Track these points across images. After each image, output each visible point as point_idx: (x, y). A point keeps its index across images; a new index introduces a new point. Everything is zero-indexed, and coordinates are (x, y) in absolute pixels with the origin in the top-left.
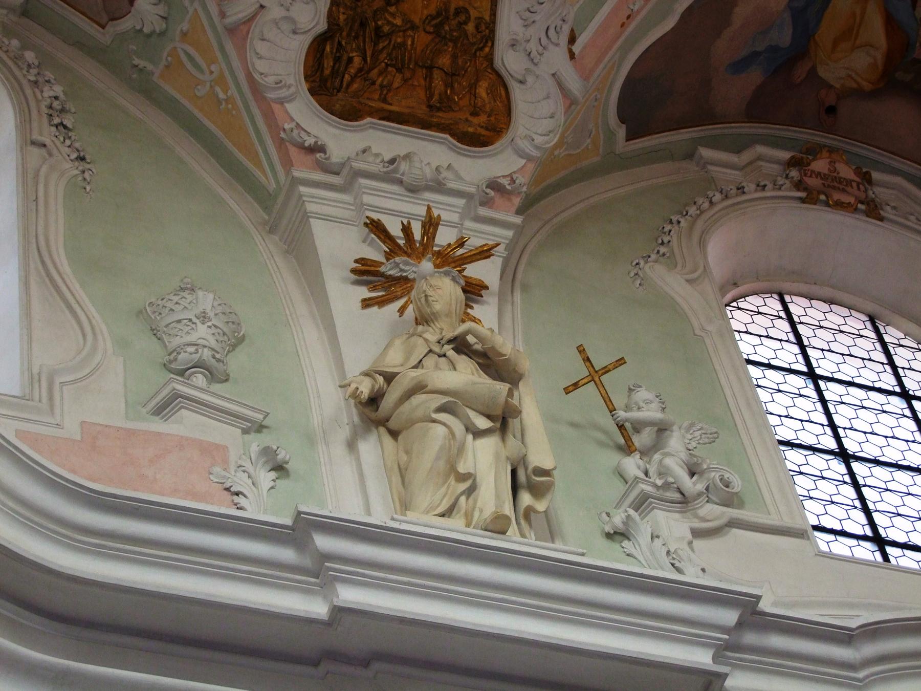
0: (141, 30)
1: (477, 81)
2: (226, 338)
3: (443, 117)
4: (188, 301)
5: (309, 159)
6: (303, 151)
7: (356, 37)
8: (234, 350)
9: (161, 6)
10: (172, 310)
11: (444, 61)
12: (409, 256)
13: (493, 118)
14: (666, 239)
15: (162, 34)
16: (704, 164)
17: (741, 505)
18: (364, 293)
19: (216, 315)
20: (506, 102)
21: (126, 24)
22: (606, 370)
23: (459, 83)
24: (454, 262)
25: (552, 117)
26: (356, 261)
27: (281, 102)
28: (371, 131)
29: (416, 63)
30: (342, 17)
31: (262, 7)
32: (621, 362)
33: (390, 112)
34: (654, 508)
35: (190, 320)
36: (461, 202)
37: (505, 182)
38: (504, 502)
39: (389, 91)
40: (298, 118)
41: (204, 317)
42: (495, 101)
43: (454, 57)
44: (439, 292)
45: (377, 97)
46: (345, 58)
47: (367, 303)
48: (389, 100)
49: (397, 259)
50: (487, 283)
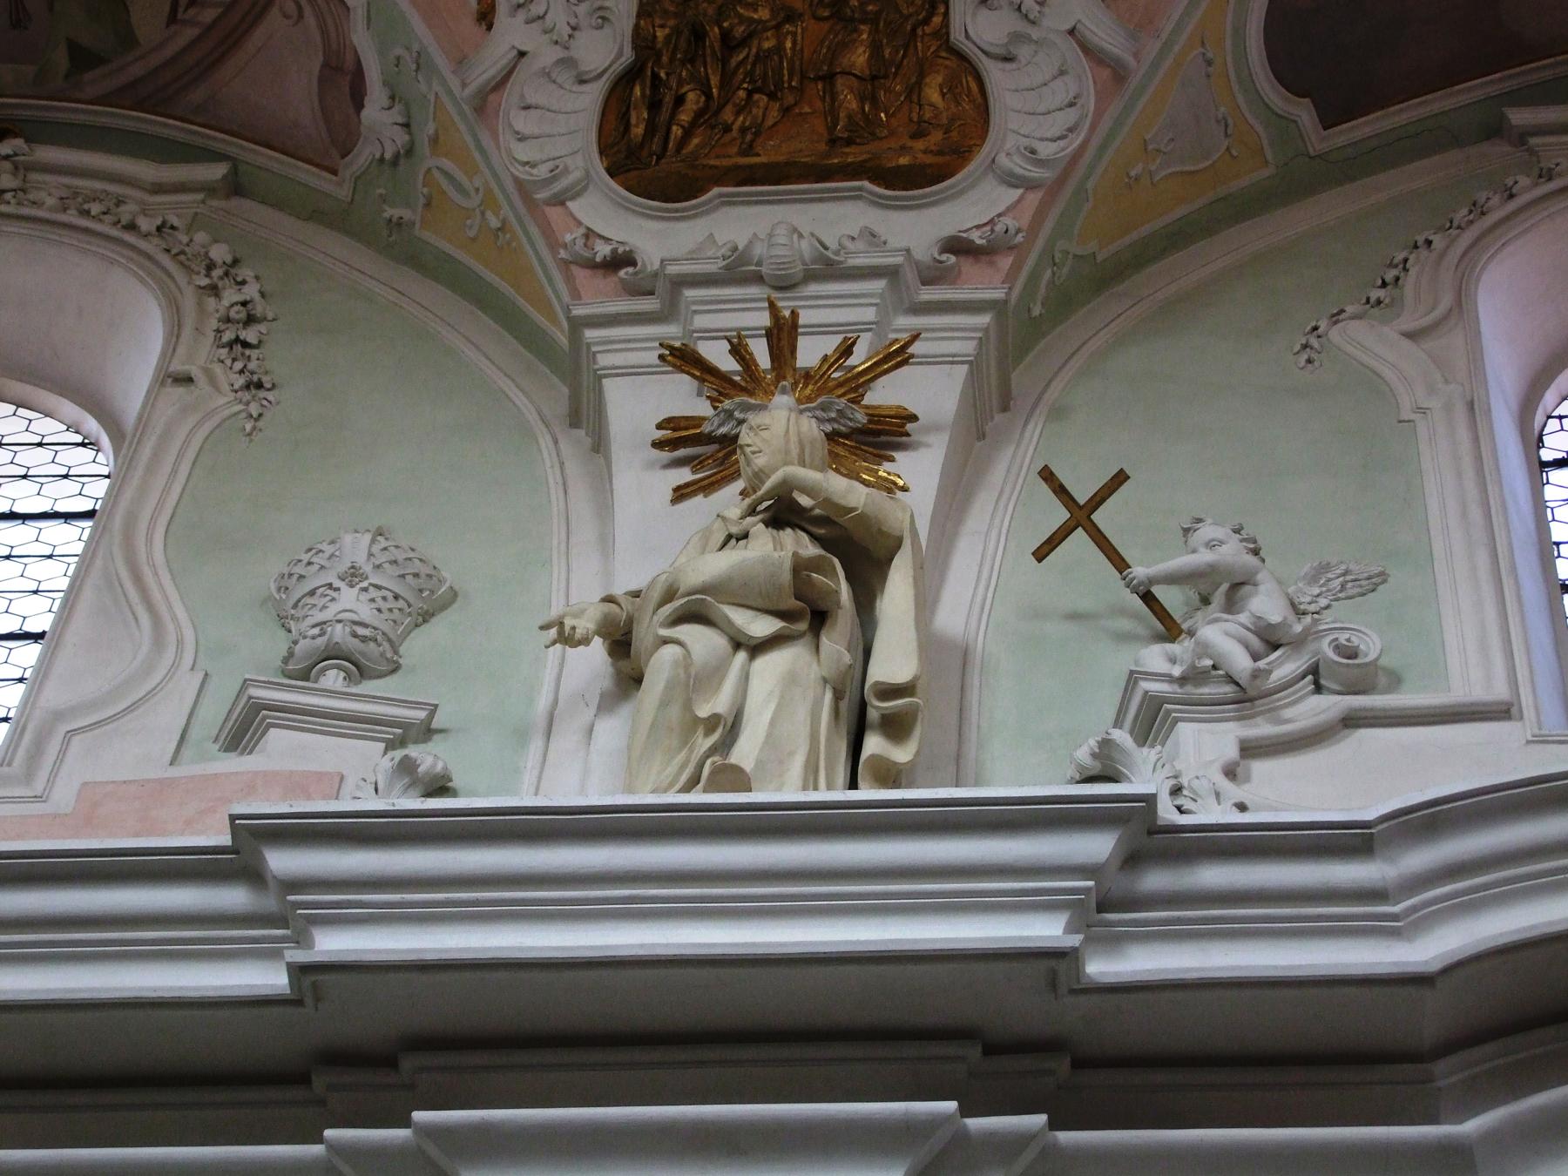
0: (382, 160)
1: (922, 75)
2: (401, 604)
3: (853, 155)
4: (327, 555)
5: (609, 283)
6: (600, 272)
7: (692, 61)
8: (425, 621)
9: (397, 107)
10: (301, 577)
11: (859, 58)
12: (751, 394)
13: (954, 134)
14: (1390, 275)
15: (410, 151)
16: (1521, 138)
17: (1395, 681)
18: (685, 475)
19: (378, 567)
20: (980, 100)
21: (364, 155)
22: (1098, 500)
23: (888, 90)
24: (840, 385)
25: (1071, 105)
26: (659, 427)
27: (560, 201)
28: (725, 209)
29: (803, 77)
30: (660, 34)
31: (522, 54)
32: (1120, 478)
33: (751, 167)
34: (1176, 720)
35: (330, 586)
36: (879, 285)
37: (977, 238)
38: (792, 754)
39: (757, 134)
40: (587, 222)
41: (353, 575)
42: (958, 104)
43: (876, 49)
44: (764, 434)
45: (735, 150)
46: (668, 99)
47: (681, 494)
48: (758, 149)
49: (727, 404)
50: (913, 409)
